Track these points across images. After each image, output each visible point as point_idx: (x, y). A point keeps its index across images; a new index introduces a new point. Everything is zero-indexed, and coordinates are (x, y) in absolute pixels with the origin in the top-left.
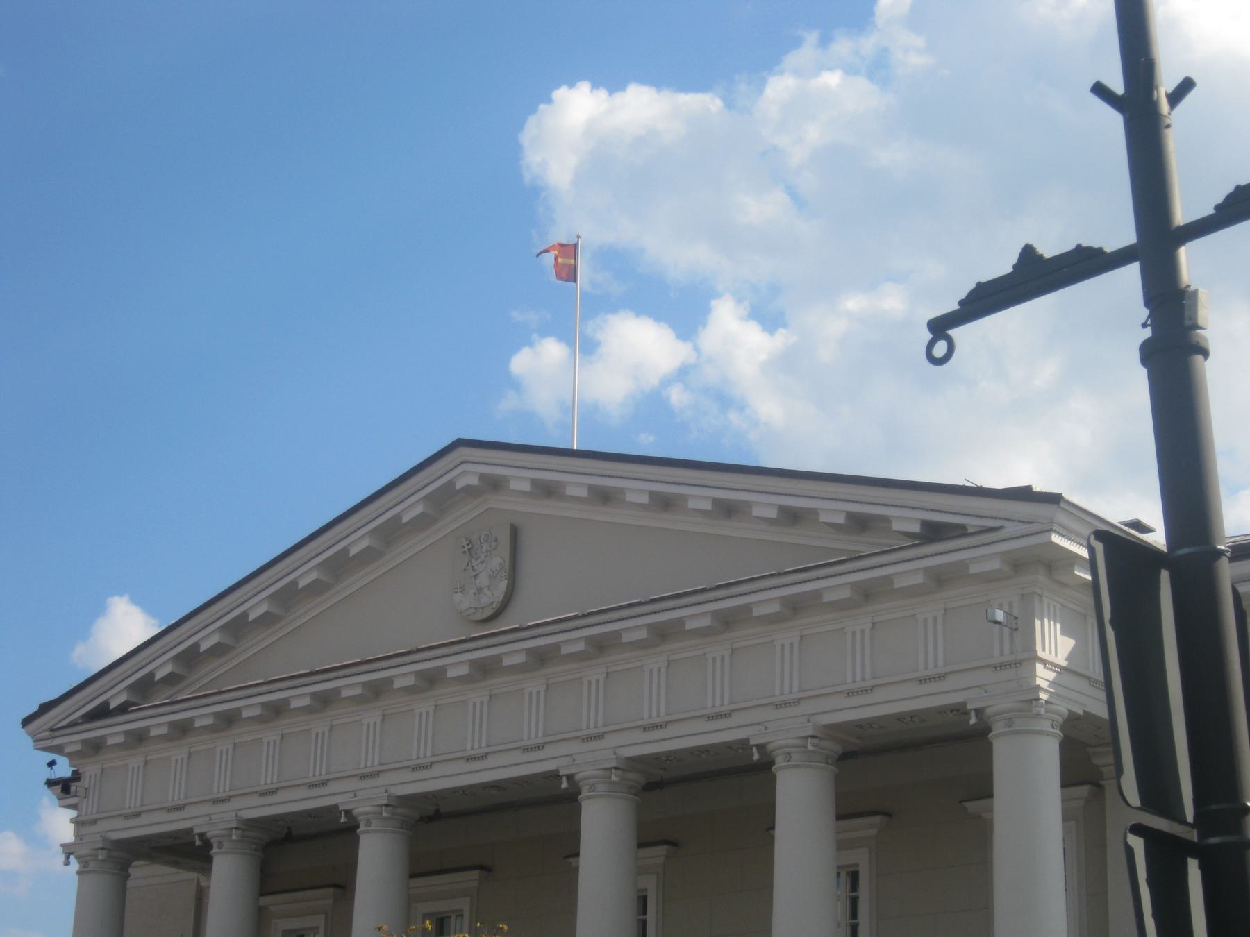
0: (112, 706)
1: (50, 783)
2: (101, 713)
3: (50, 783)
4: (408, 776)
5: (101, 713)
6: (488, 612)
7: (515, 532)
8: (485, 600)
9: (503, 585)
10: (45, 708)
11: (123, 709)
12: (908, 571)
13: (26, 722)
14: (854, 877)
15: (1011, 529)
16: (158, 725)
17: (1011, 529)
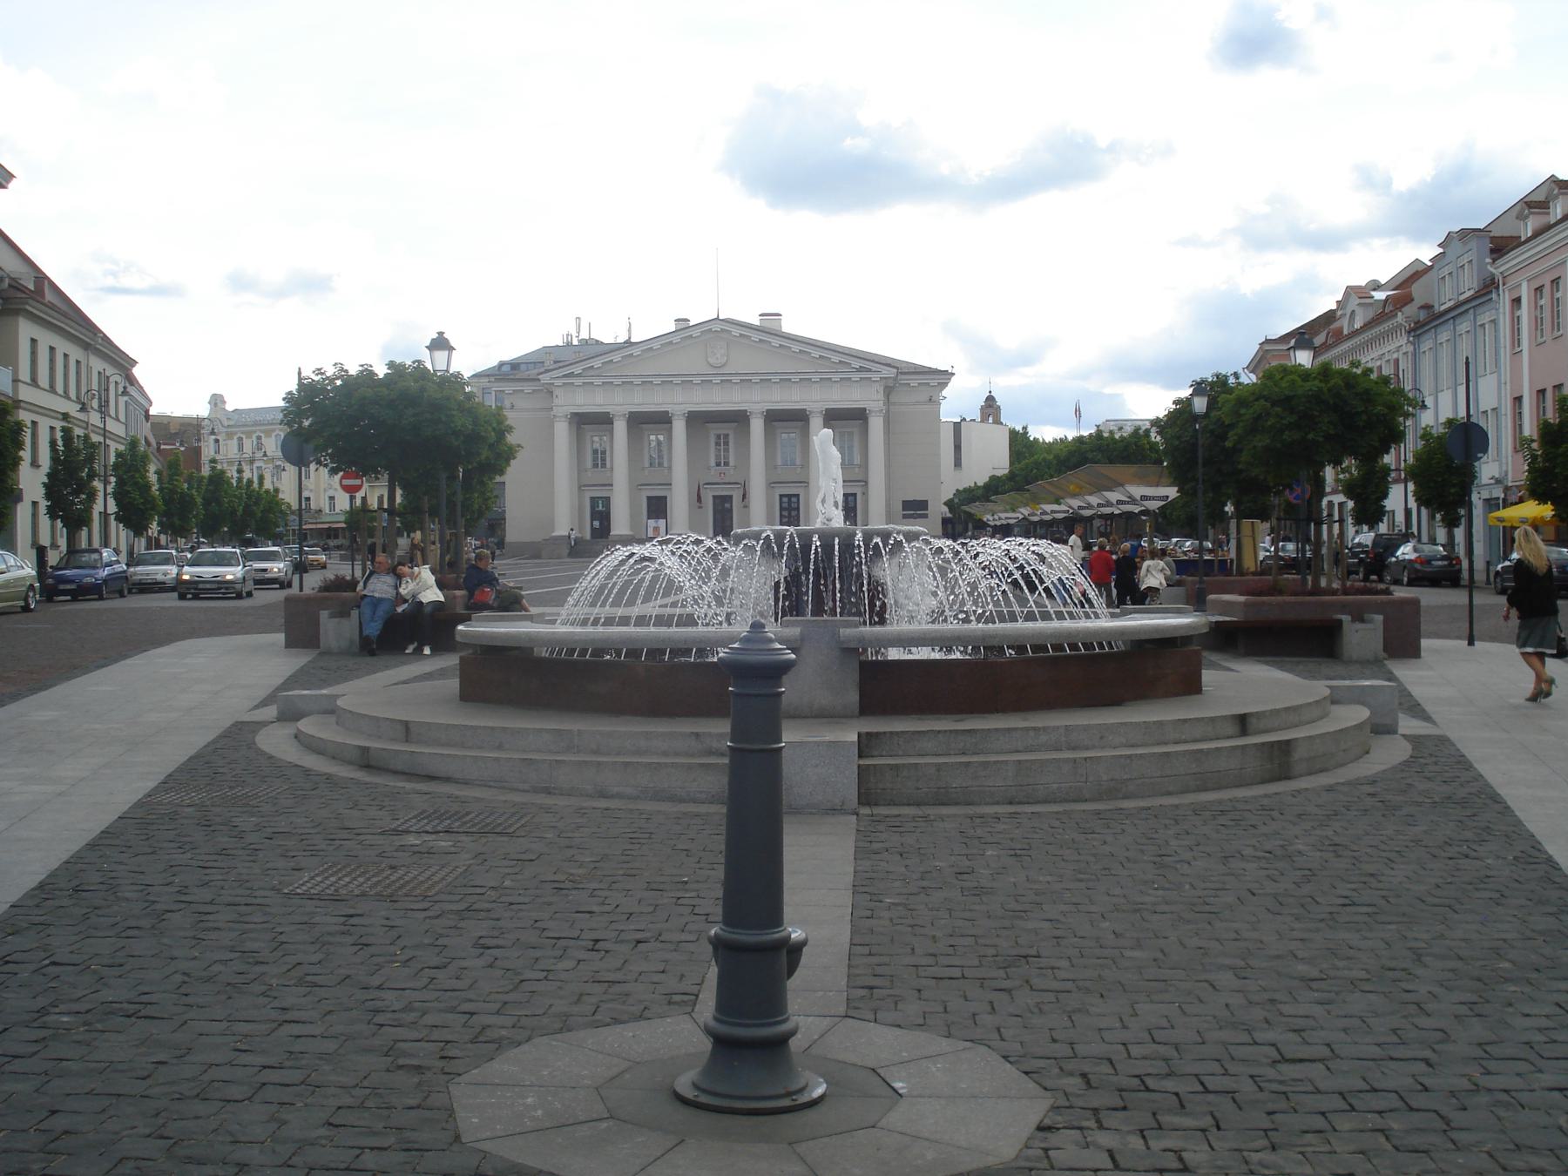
2: (571, 375)
5: (571, 375)
11: (579, 375)
12: (856, 377)
16: (598, 381)
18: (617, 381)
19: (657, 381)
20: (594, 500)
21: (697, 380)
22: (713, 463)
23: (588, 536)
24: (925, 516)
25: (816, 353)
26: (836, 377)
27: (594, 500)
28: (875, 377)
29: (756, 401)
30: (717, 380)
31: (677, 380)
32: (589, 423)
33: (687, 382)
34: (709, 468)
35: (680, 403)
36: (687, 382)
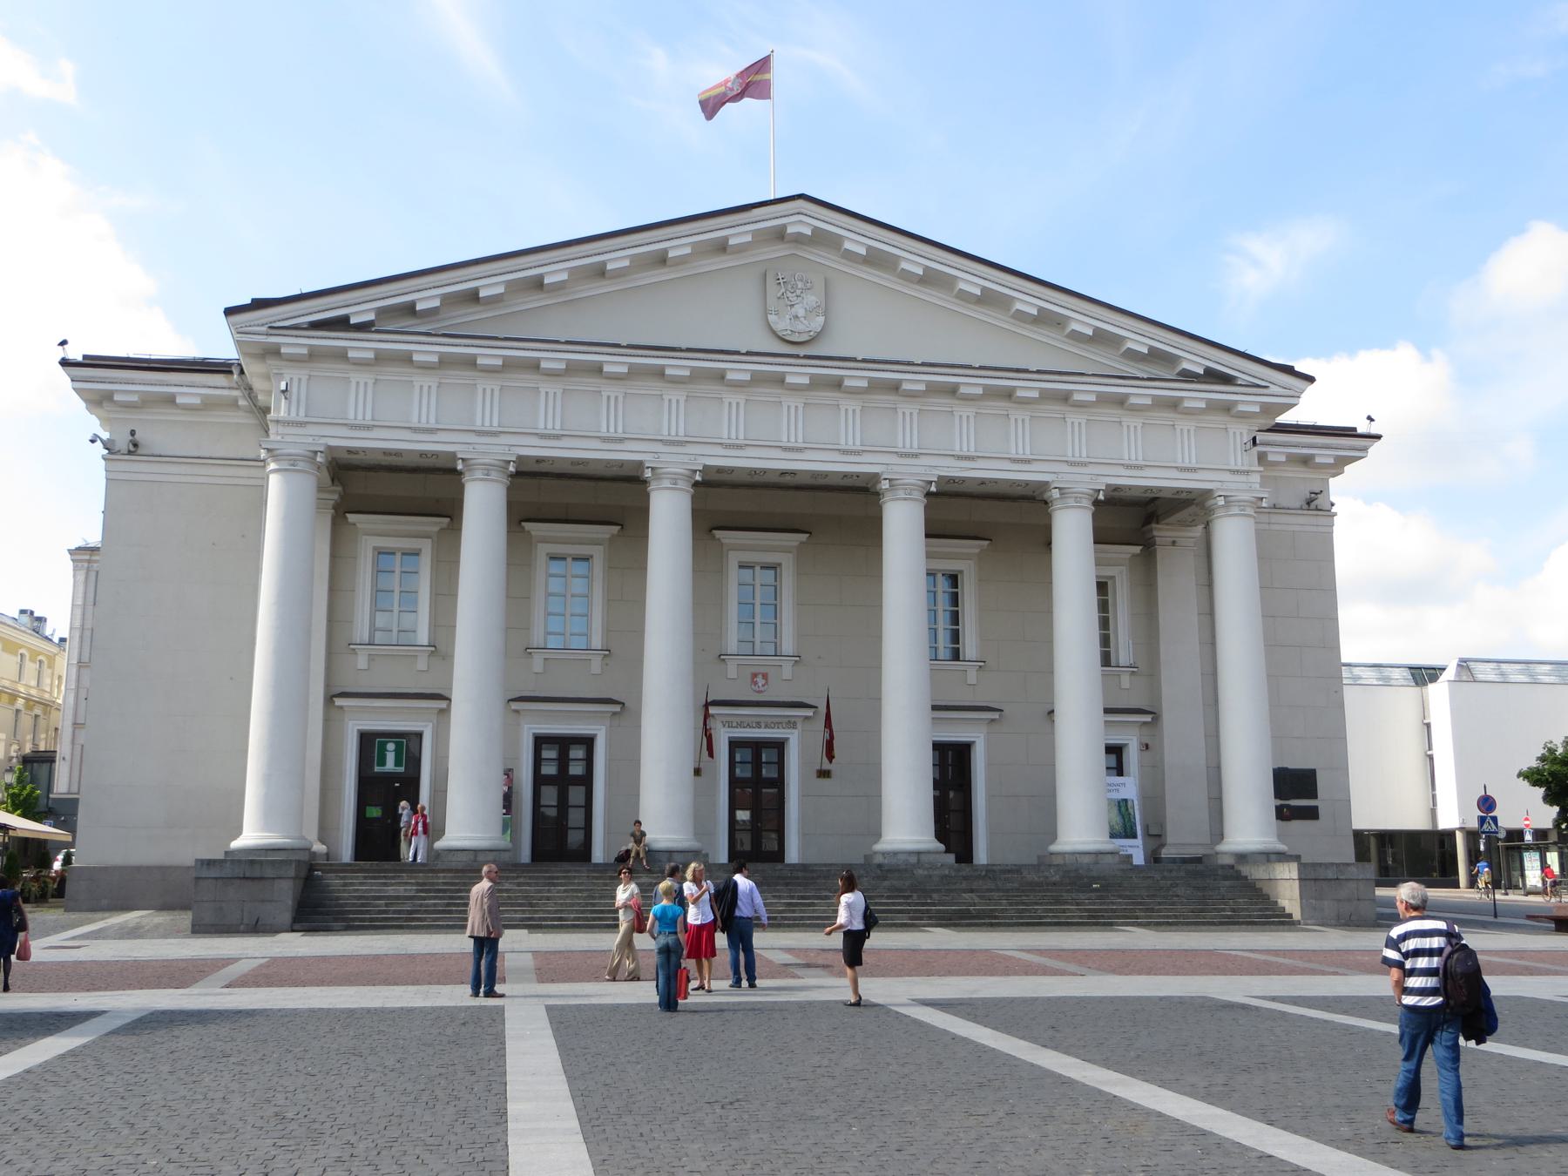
0: (353, 321)
1: (65, 363)
2: (341, 324)
3: (65, 363)
4: (720, 451)
5: (341, 324)
6: (804, 338)
7: (826, 280)
8: (800, 327)
9: (821, 319)
10: (259, 304)
11: (364, 327)
12: (1196, 396)
13: (229, 312)
14: (954, 579)
15: (1274, 389)
16: (426, 352)
17: (1274, 389)
18: (489, 356)
19: (616, 364)
20: (369, 743)
21: (738, 371)
22: (732, 645)
23: (346, 852)
24: (1312, 814)
25: (1083, 324)
26: (1141, 395)
27: (369, 743)
28: (1249, 403)
29: (908, 452)
30: (798, 375)
31: (677, 367)
32: (387, 494)
33: (709, 369)
34: (721, 657)
35: (673, 437)
36: (709, 369)
